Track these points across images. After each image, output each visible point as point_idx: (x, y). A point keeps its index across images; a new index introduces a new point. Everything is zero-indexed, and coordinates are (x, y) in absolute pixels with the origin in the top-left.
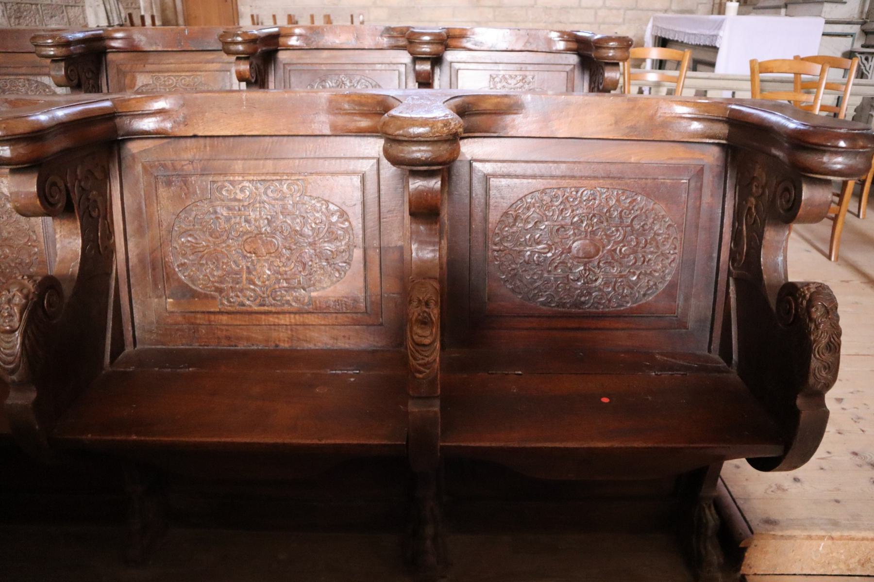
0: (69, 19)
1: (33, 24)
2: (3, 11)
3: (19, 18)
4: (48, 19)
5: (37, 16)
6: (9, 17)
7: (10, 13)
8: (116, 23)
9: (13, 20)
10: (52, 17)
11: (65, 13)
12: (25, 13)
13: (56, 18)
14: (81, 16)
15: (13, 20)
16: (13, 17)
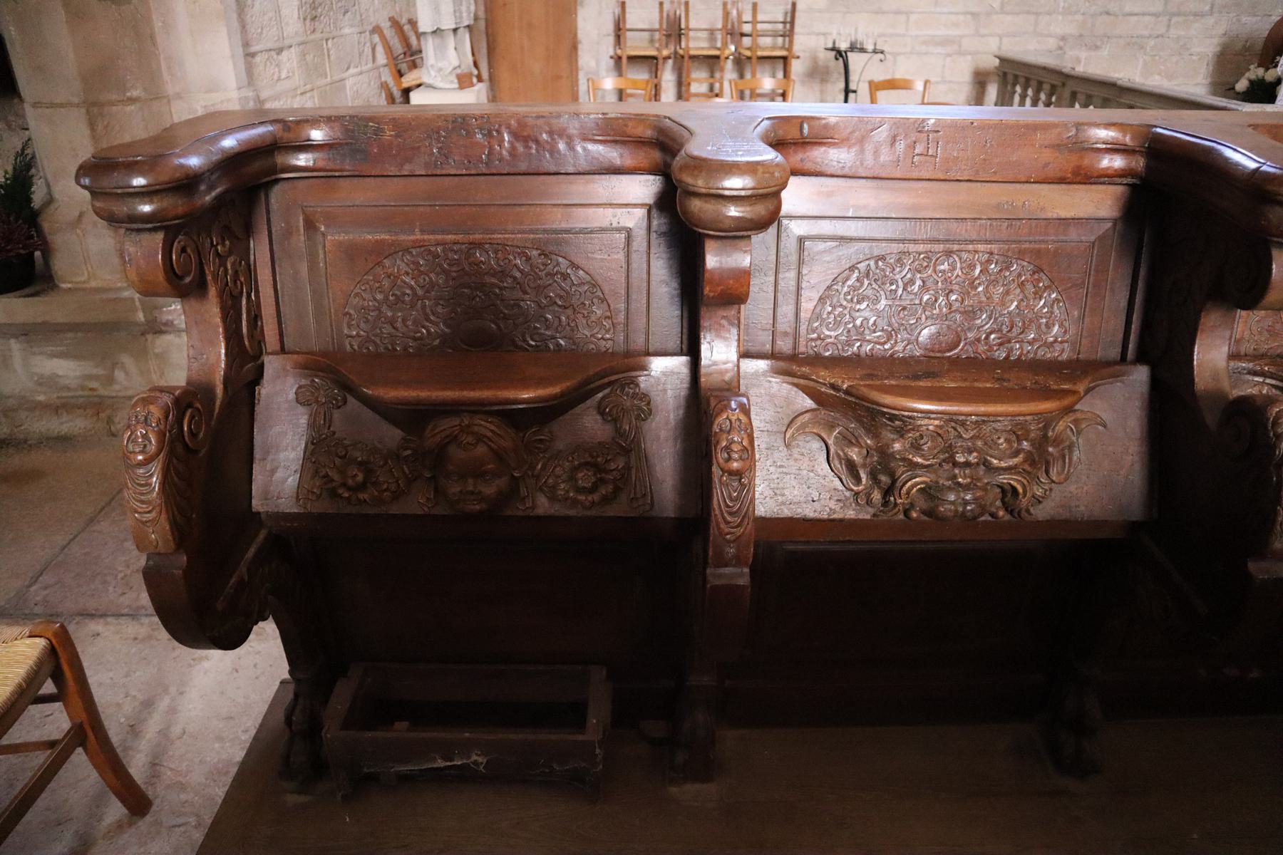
0: (361, 16)
1: (328, 30)
2: (299, 9)
3: (313, 19)
4: (342, 17)
5: (332, 13)
6: (305, 19)
7: (306, 11)
8: (466, 23)
9: (308, 22)
10: (344, 15)
11: (356, 7)
12: (320, 10)
13: (349, 13)
14: (371, 10)
15: (308, 22)
16: (309, 17)
